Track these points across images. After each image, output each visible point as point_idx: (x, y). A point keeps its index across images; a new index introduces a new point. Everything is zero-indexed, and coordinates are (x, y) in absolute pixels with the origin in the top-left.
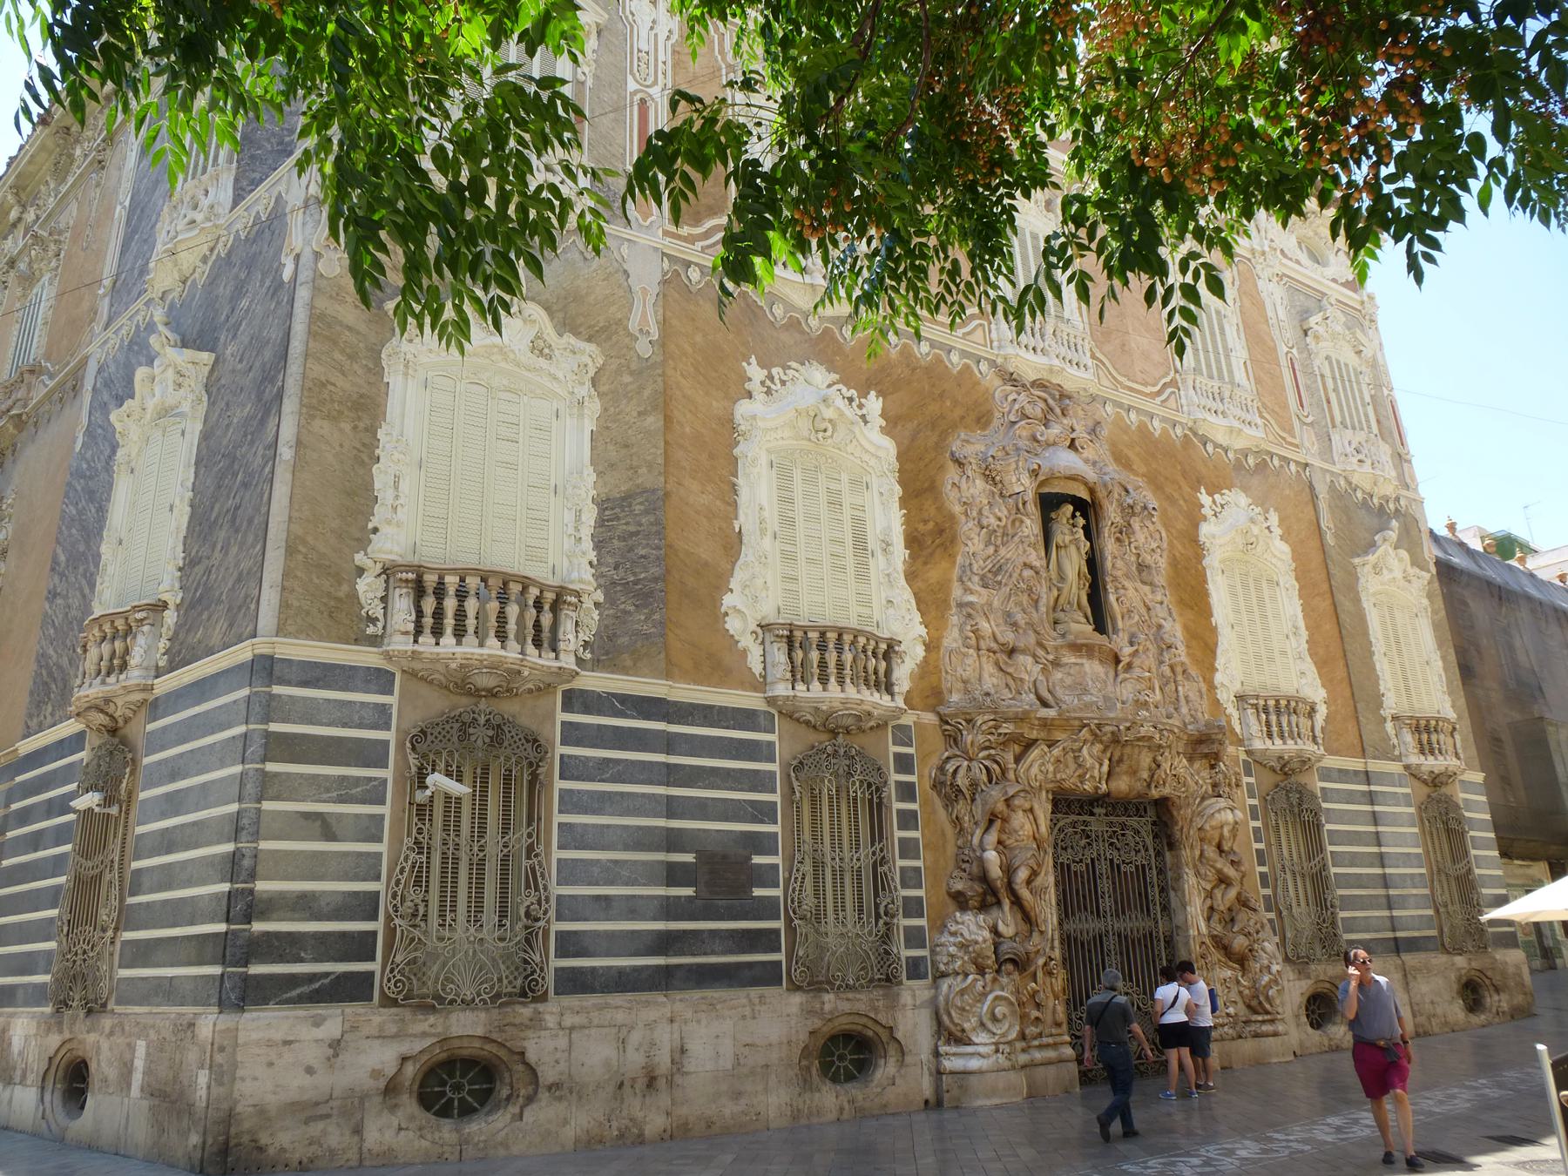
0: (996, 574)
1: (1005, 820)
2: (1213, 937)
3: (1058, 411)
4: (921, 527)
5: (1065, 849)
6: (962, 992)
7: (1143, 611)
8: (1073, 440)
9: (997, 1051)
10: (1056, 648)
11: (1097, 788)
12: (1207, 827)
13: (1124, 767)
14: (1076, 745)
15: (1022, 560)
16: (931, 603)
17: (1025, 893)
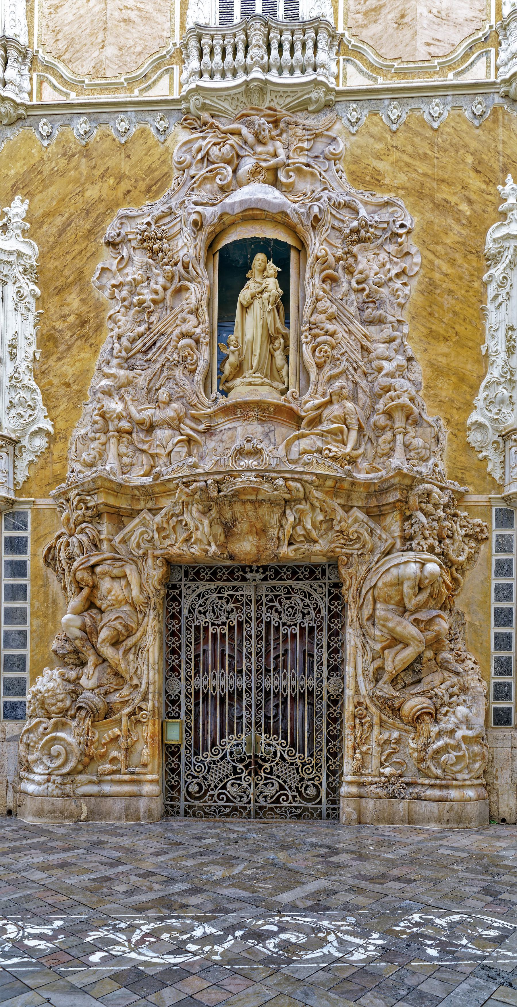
10: (209, 417)
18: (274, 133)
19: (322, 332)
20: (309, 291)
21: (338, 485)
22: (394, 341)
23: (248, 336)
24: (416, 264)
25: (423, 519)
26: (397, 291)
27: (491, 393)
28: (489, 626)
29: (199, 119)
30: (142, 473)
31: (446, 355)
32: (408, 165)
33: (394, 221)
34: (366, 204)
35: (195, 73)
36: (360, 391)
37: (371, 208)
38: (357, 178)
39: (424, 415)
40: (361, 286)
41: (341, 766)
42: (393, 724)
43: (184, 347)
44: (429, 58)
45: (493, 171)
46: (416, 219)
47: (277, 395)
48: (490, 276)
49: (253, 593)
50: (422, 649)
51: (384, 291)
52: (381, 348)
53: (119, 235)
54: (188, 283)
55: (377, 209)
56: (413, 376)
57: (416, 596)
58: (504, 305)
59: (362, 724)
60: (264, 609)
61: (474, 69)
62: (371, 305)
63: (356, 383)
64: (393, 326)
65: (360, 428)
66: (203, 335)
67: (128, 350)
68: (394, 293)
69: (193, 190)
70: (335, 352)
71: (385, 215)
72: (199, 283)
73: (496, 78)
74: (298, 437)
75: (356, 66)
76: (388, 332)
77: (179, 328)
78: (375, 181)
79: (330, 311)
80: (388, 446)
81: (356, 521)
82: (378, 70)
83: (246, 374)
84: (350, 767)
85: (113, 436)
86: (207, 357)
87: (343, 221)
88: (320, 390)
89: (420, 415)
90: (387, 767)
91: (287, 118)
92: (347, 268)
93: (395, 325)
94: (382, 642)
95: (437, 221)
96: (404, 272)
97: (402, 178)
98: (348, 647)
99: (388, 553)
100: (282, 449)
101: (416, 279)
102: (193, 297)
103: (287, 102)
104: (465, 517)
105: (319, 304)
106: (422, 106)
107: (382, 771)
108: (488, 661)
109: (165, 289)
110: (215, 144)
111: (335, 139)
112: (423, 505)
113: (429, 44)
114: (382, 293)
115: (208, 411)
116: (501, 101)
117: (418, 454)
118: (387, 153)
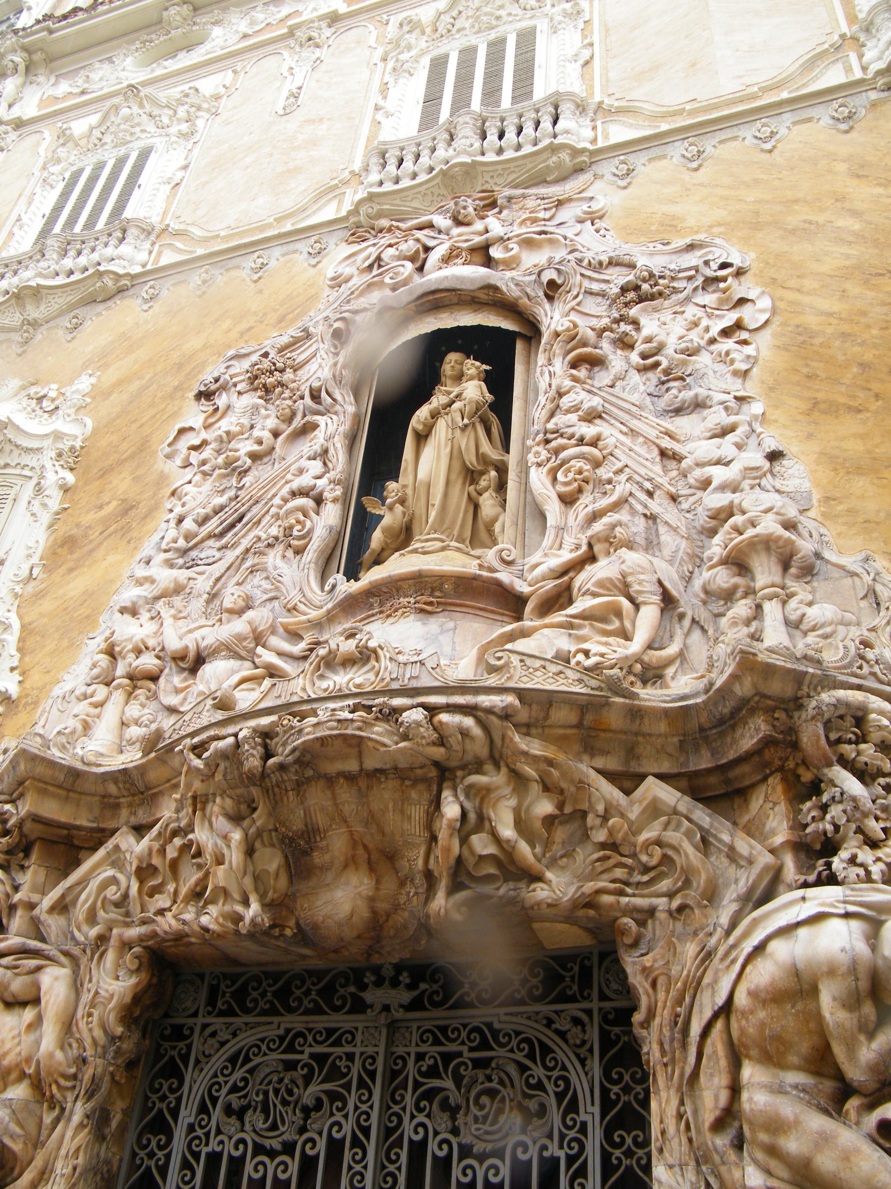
0: (222, 534)
5: (240, 1114)
8: (484, 248)
11: (239, 918)
12: (741, 999)
13: (337, 844)
19: (573, 441)
20: (543, 384)
26: (727, 354)
31: (862, 437)
32: (726, 198)
36: (662, 529)
39: (827, 555)
40: (650, 361)
43: (288, 513)
46: (753, 255)
49: (381, 1049)
53: (217, 380)
55: (674, 257)
56: (790, 485)
60: (409, 1100)
63: (652, 518)
64: (726, 409)
67: (188, 537)
72: (336, 413)
76: (716, 417)
77: (288, 487)
79: (585, 406)
80: (745, 631)
89: (818, 555)
93: (733, 404)
96: (738, 326)
97: (720, 214)
103: (509, 179)
105: (565, 399)
106: (740, 133)
109: (276, 434)
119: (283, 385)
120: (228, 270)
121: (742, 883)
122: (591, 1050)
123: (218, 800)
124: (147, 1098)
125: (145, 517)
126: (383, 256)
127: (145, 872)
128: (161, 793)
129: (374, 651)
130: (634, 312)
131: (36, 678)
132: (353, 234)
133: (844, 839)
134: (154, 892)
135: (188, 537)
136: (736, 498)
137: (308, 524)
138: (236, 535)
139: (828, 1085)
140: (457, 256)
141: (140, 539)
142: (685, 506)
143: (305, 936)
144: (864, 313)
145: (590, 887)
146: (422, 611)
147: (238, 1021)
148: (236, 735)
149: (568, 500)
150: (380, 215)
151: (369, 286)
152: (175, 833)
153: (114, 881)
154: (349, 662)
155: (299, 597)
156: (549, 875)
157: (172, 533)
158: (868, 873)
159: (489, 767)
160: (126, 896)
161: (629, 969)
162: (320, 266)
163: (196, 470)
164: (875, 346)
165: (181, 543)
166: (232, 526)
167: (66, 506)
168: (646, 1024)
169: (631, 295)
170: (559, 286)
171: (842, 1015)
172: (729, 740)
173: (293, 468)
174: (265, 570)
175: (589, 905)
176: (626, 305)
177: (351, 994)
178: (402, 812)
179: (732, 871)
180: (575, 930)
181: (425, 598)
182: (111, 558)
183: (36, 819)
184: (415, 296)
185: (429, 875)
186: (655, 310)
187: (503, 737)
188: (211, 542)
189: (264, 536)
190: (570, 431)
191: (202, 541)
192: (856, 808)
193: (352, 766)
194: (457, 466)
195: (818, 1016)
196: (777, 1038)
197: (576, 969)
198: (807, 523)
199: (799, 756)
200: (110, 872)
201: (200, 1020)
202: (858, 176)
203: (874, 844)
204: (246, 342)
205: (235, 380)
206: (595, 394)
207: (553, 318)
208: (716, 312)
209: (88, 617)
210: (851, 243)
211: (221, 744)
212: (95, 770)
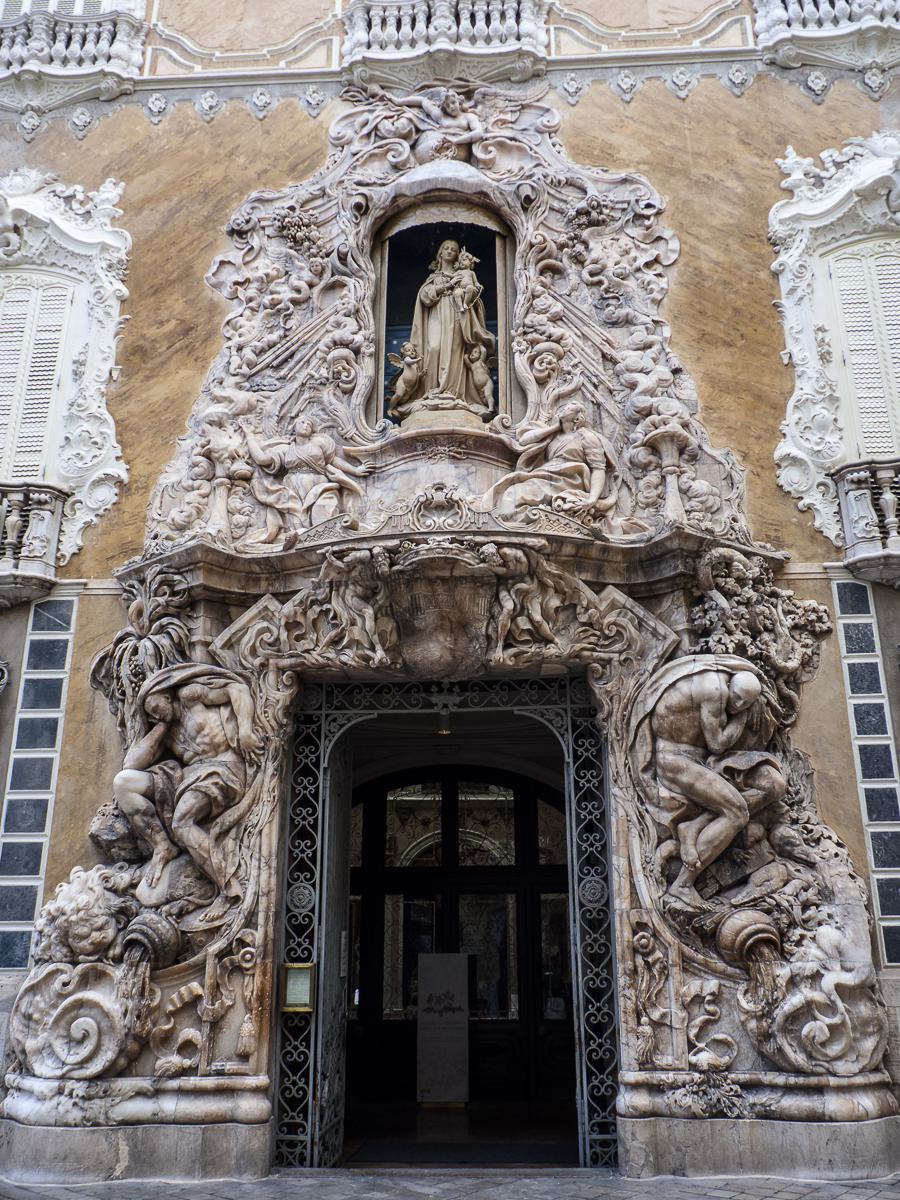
0: (278, 368)
1: (174, 723)
2: (670, 914)
3: (436, 111)
4: (153, 332)
6: (33, 989)
7: (598, 368)
9: (60, 1092)
10: (373, 454)
11: (367, 659)
12: (661, 709)
14: (321, 595)
15: (327, 339)
16: (143, 429)
17: (193, 836)
18: (466, 105)
19: (544, 337)
20: (521, 285)
21: (581, 551)
22: (650, 347)
23: (433, 343)
24: (673, 251)
25: (723, 602)
26: (649, 284)
27: (805, 415)
28: (853, 777)
29: (365, 91)
30: (264, 537)
31: (731, 366)
32: (648, 137)
33: (637, 201)
34: (596, 181)
35: (361, 45)
36: (604, 415)
37: (604, 187)
38: (580, 153)
39: (705, 447)
40: (596, 279)
41: (614, 1052)
42: (706, 964)
43: (336, 360)
44: (666, 25)
45: (766, 143)
46: (667, 198)
47: (478, 421)
48: (781, 265)
50: (742, 821)
51: (631, 284)
52: (632, 358)
53: (248, 222)
54: (344, 278)
55: (612, 186)
56: (685, 394)
57: (724, 729)
58: (806, 299)
59: (649, 966)
61: (727, 36)
62: (613, 302)
63: (598, 405)
64: (647, 329)
65: (609, 467)
66: (367, 343)
67: (250, 365)
68: (646, 286)
69: (355, 168)
70: (563, 363)
71: (624, 193)
72: (360, 277)
73: (756, 44)
74: (512, 482)
75: (572, 34)
76: (640, 335)
77: (330, 335)
78: (604, 156)
79: (553, 310)
80: (655, 493)
81: (613, 606)
82: (601, 38)
83: (430, 394)
84: (633, 1054)
85: (221, 484)
86: (371, 372)
87: (565, 201)
88: (544, 415)
89: (700, 447)
90: (701, 1050)
91: (483, 90)
92: (575, 257)
93: (651, 326)
94: (671, 810)
95: (696, 200)
96: (656, 260)
97: (645, 152)
98: (613, 820)
99: (671, 657)
100: (488, 495)
101: (675, 269)
102: (352, 295)
104: (789, 598)
105: (536, 301)
106: (662, 74)
107: (693, 1059)
108: (862, 842)
109: (311, 286)
110: (386, 118)
111: (548, 110)
112: (721, 581)
113: (664, 12)
114: (627, 286)
115: (371, 446)
116: (765, 68)
117: (702, 502)
118: (620, 124)
119: (309, 240)
120: (231, 99)
121: (660, 648)
122: (567, 730)
123: (351, 587)
124: (295, 757)
125: (206, 340)
126: (379, 126)
127: (291, 625)
128: (295, 574)
129: (457, 502)
130: (585, 233)
131: (141, 468)
132: (346, 92)
133: (715, 629)
134: (298, 638)
135: (250, 365)
136: (654, 400)
137: (353, 372)
138: (291, 369)
139: (700, 751)
140: (448, 148)
141: (205, 359)
142: (618, 398)
143: (406, 667)
144: (739, 267)
145: (578, 646)
146: (454, 457)
147: (350, 712)
148: (370, 550)
149: (541, 383)
150: (372, 79)
151: (371, 155)
152: (313, 603)
153: (268, 630)
154: (440, 508)
155: (354, 430)
156: (556, 640)
157: (236, 360)
158: (727, 648)
159: (528, 579)
160: (278, 639)
161: (597, 691)
162: (320, 118)
163: (244, 306)
164: (744, 296)
165: (245, 370)
166: (285, 361)
167: (128, 317)
168: (605, 720)
169: (584, 219)
170: (532, 201)
171: (713, 720)
172: (655, 568)
173: (332, 319)
174: (321, 403)
175: (577, 656)
176: (580, 226)
177: (423, 698)
178: (474, 601)
179: (654, 642)
180: (564, 667)
181: (455, 449)
182: (183, 373)
183: (205, 588)
184: (424, 190)
185: (488, 637)
186: (600, 235)
187: (538, 563)
188: (269, 372)
189: (317, 376)
190: (542, 328)
191: (262, 369)
192: (724, 614)
193: (446, 574)
194: (458, 340)
195: (700, 720)
196: (679, 729)
197: (556, 686)
198: (695, 425)
199: (695, 582)
200: (265, 624)
201: (324, 712)
202: (744, 143)
203: (730, 633)
204: (265, 184)
205: (263, 223)
206: (557, 300)
207: (529, 230)
208: (643, 246)
209: (174, 421)
210: (734, 203)
211: (358, 554)
212: (244, 556)
